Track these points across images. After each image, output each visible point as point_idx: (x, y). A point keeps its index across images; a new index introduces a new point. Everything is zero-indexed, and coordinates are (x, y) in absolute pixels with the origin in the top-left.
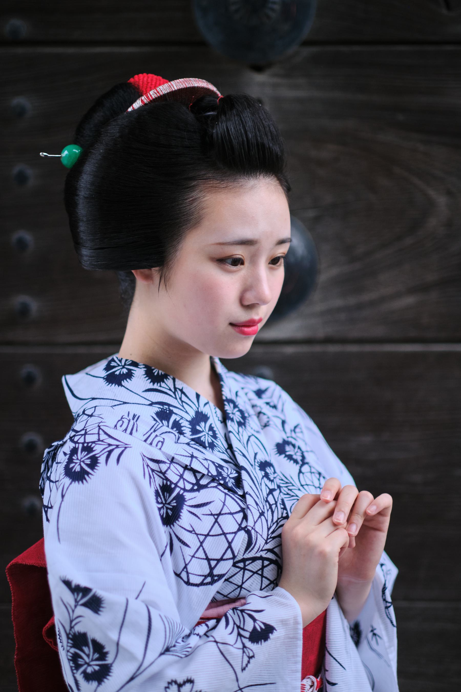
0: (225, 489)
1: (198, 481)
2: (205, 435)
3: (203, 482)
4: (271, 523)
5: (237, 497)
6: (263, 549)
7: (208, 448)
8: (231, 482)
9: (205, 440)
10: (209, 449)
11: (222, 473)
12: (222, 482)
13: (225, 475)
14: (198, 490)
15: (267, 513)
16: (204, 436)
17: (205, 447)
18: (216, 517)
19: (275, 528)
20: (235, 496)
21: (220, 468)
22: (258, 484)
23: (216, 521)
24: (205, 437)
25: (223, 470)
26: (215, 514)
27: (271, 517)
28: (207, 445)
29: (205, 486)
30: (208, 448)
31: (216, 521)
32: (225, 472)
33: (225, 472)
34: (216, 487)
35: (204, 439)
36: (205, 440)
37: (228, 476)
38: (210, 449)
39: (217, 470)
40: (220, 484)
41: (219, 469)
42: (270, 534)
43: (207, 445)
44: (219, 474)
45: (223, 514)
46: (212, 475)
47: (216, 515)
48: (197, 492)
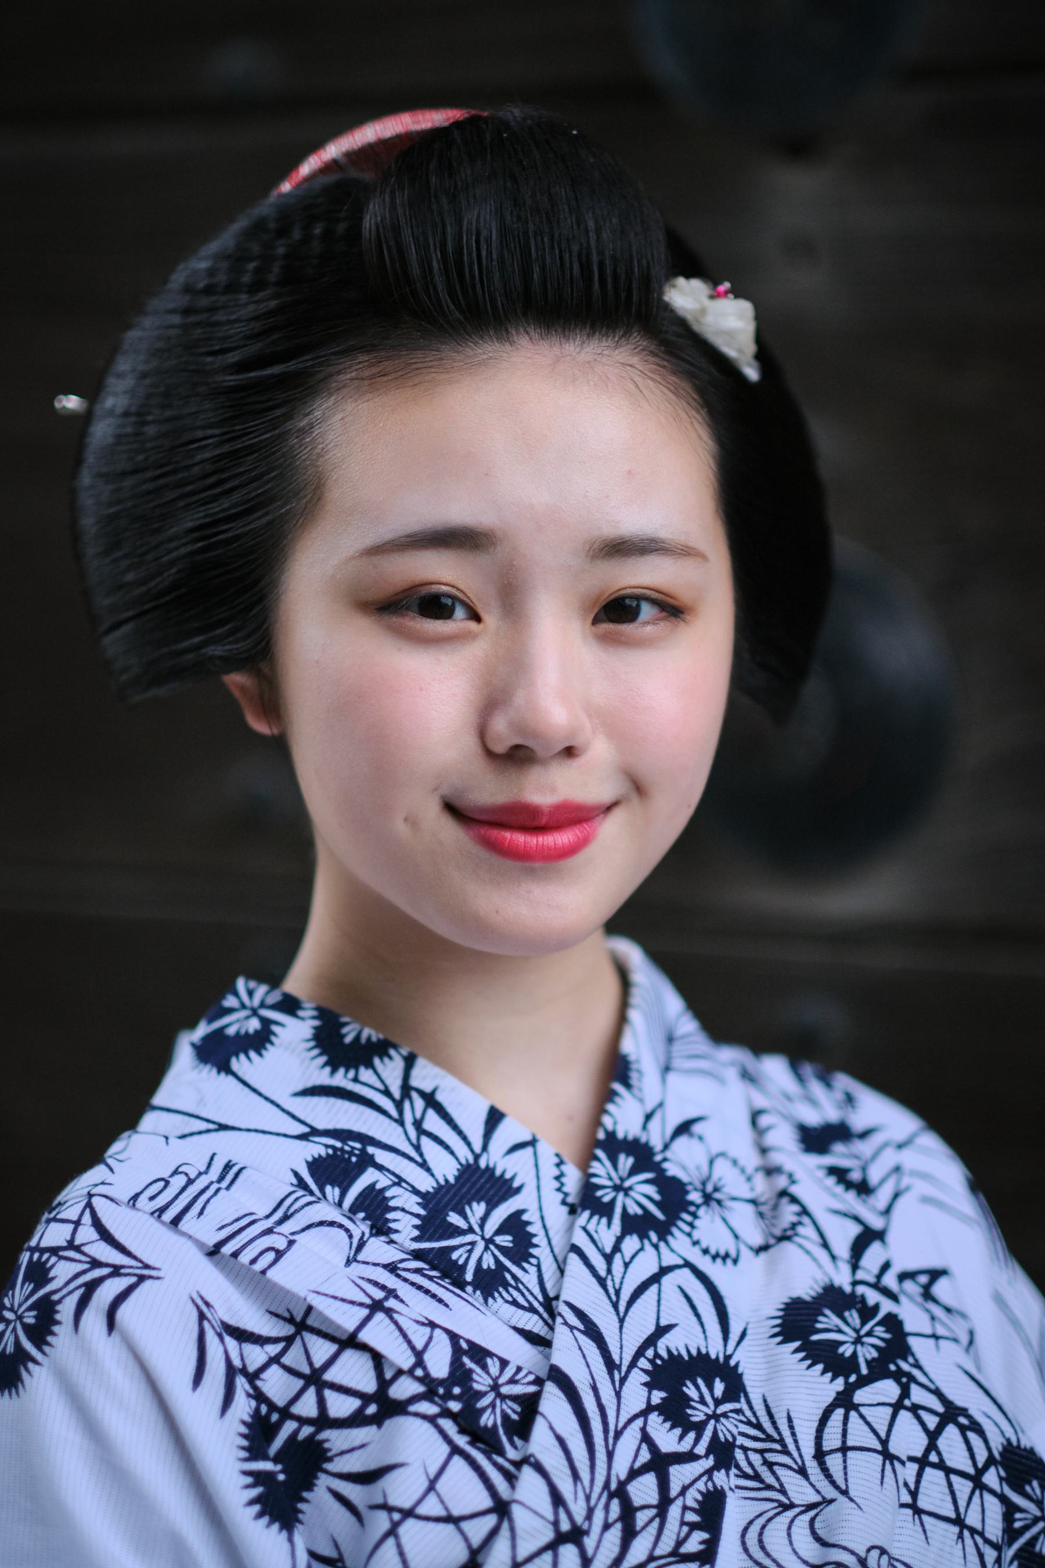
7: (469, 1289)
10: (474, 1292)
17: (461, 1284)
28: (469, 1277)
30: (469, 1289)
38: (478, 1293)
43: (469, 1277)
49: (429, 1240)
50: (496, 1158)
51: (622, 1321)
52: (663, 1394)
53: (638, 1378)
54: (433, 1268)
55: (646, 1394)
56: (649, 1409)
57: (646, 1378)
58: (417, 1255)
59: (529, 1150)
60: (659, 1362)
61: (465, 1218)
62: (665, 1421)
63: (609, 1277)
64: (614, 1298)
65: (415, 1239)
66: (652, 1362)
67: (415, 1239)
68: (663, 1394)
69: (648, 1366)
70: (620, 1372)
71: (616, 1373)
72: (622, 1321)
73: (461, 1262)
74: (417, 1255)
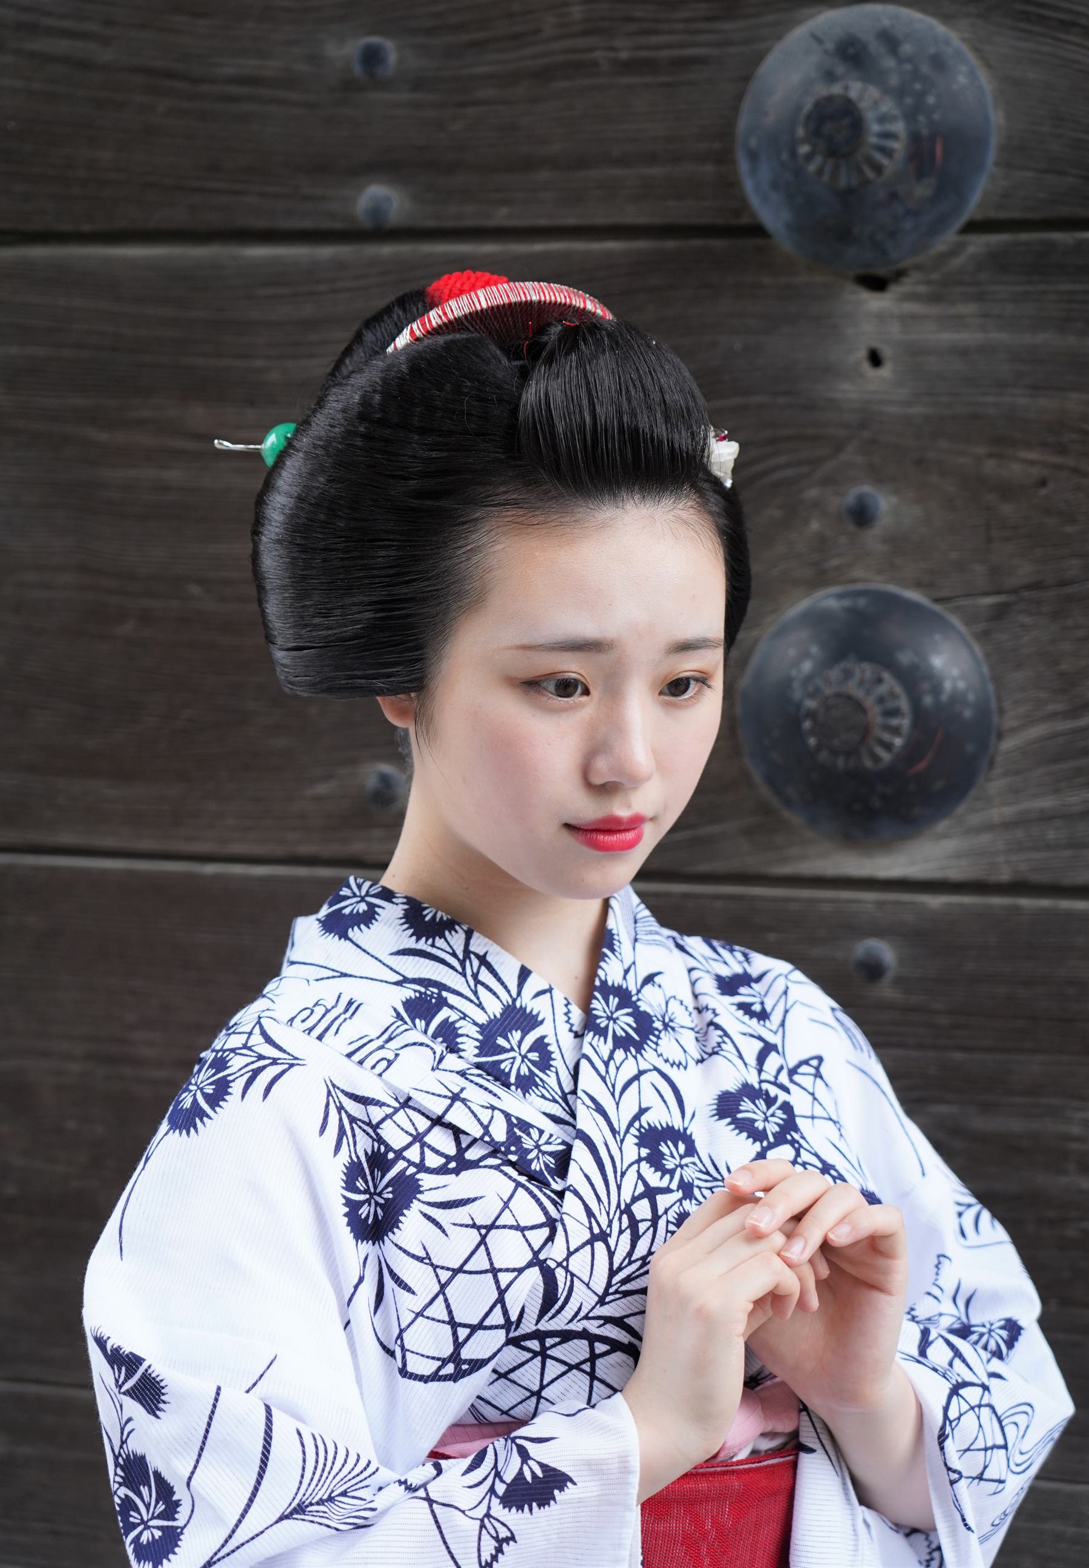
0: (521, 1174)
1: (461, 1151)
2: (514, 1058)
3: (472, 1155)
4: (624, 1260)
5: (545, 1194)
6: (591, 1315)
8: (544, 1161)
9: (511, 1068)
10: (517, 1090)
11: (523, 1140)
12: (513, 1158)
13: (528, 1143)
14: (457, 1172)
15: (618, 1237)
16: (512, 1060)
18: (483, 1231)
19: (634, 1272)
20: (541, 1191)
21: (520, 1129)
22: (615, 1172)
23: (483, 1241)
24: (513, 1063)
25: (529, 1134)
26: (482, 1225)
27: (628, 1247)
28: (512, 1080)
29: (474, 1164)
30: (513, 1088)
31: (483, 1241)
32: (531, 1138)
33: (531, 1138)
34: (497, 1168)
35: (509, 1066)
36: (511, 1068)
37: (538, 1147)
38: (519, 1090)
39: (510, 1132)
40: (513, 1164)
41: (516, 1130)
42: (617, 1283)
43: (512, 1080)
44: (513, 1139)
45: (498, 1227)
46: (493, 1140)
47: (485, 1227)
48: (454, 1176)
49: (485, 1056)
50: (526, 1000)
51: (617, 1104)
52: (648, 1151)
53: (631, 1141)
54: (489, 1074)
55: (637, 1150)
56: (639, 1160)
57: (637, 1141)
58: (478, 1066)
59: (548, 995)
60: (643, 1130)
61: (508, 1041)
62: (651, 1167)
63: (607, 1076)
64: (612, 1090)
65: (476, 1056)
66: (639, 1130)
67: (476, 1056)
68: (648, 1151)
69: (637, 1134)
70: (619, 1136)
71: (617, 1136)
72: (617, 1104)
73: (507, 1070)
74: (478, 1066)
